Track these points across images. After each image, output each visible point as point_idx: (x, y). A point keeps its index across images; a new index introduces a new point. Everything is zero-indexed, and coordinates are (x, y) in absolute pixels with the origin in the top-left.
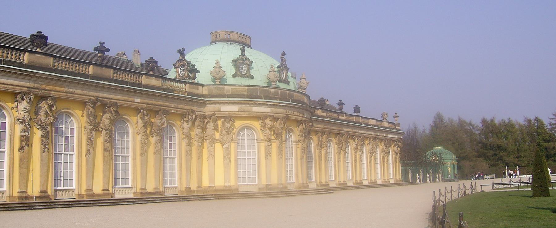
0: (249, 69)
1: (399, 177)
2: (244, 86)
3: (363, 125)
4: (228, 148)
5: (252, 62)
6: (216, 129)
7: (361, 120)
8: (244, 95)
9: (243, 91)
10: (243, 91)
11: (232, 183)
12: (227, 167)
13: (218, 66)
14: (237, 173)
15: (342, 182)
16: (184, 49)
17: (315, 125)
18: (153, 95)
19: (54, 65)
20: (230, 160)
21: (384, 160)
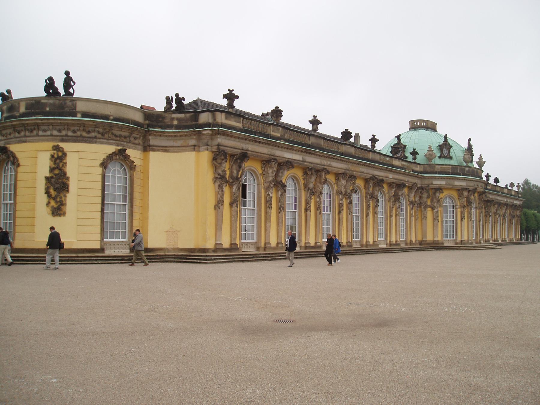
0: (449, 152)
2: (449, 165)
4: (437, 212)
6: (428, 197)
7: (499, 189)
8: (449, 172)
11: (438, 238)
12: (435, 226)
13: (430, 150)
14: (442, 231)
16: (400, 135)
18: (399, 173)
19: (355, 153)
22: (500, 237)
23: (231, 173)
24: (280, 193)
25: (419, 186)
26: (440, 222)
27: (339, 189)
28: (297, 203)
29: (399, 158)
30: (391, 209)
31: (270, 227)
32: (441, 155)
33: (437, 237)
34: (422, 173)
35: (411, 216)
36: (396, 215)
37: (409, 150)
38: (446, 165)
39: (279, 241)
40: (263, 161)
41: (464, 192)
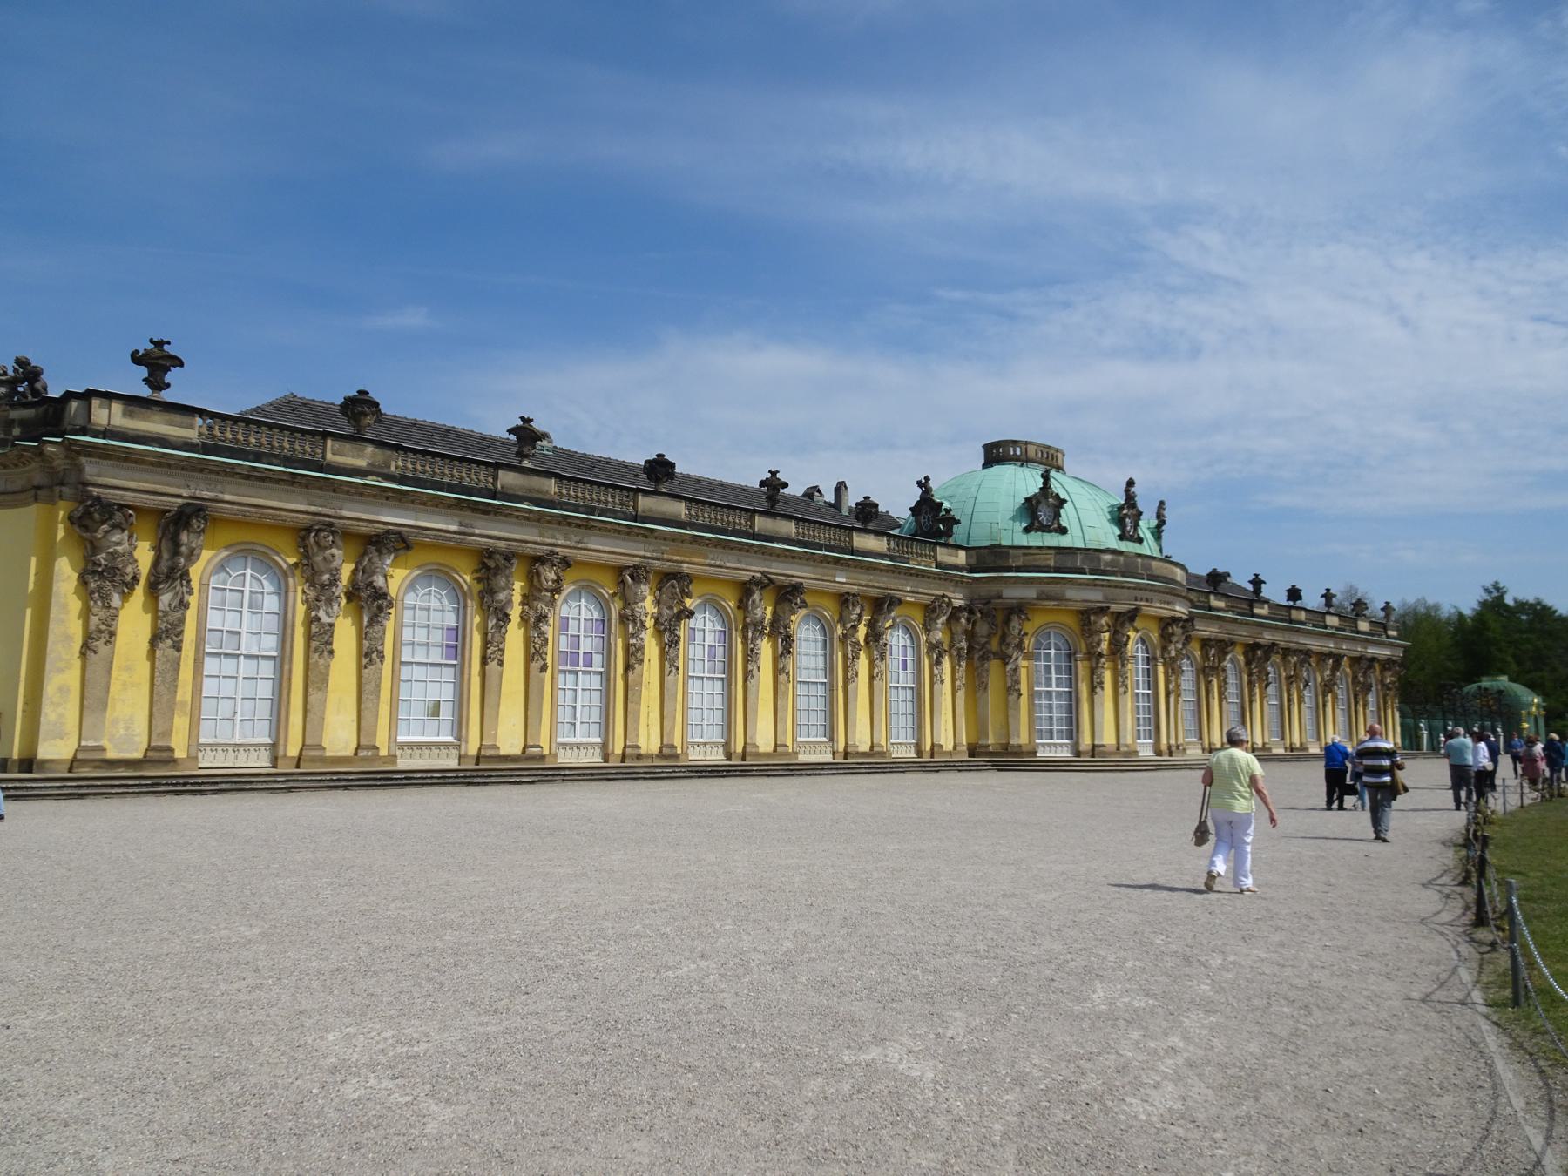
0: (1058, 515)
4: (1016, 670)
5: (1065, 501)
14: (1032, 721)
23: (156, 563)
25: (957, 603)
36: (872, 678)
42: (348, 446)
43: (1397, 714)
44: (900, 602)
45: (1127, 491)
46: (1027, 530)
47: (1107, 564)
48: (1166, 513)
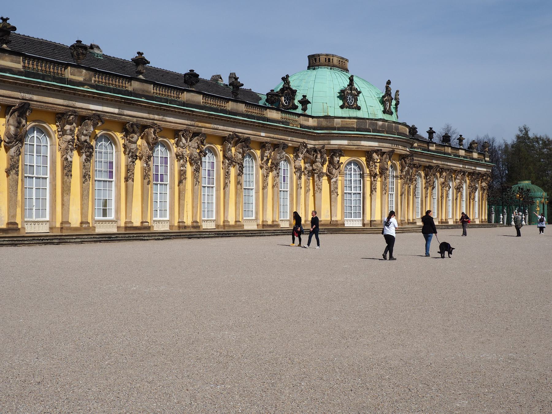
1: (485, 217)
3: (452, 156)
4: (336, 182)
5: (360, 92)
7: (449, 150)
8: (354, 128)
9: (353, 124)
10: (353, 124)
11: (338, 217)
15: (411, 221)
16: (288, 76)
17: (415, 158)
20: (338, 195)
21: (470, 197)
22: (453, 218)
24: (84, 156)
25: (309, 146)
26: (339, 197)
27: (179, 151)
28: (114, 170)
29: (278, 109)
30: (265, 177)
31: (69, 200)
32: (344, 104)
33: (336, 216)
34: (315, 128)
35: (299, 187)
36: (273, 186)
37: (298, 97)
38: (350, 118)
39: (84, 220)
40: (58, 114)
41: (375, 156)
42: (76, 70)
43: (487, 203)
44: (288, 146)
45: (387, 88)
46: (342, 107)
47: (380, 127)
48: (399, 97)
